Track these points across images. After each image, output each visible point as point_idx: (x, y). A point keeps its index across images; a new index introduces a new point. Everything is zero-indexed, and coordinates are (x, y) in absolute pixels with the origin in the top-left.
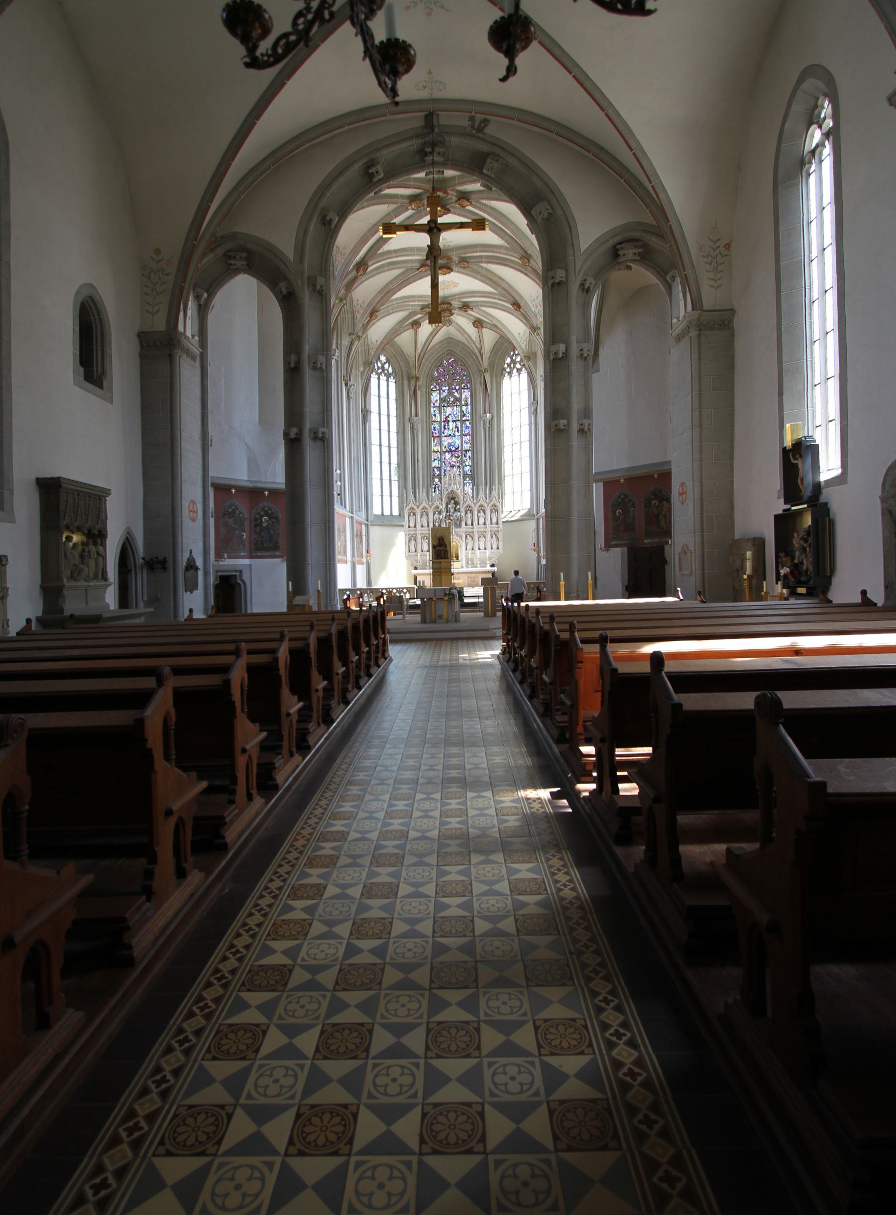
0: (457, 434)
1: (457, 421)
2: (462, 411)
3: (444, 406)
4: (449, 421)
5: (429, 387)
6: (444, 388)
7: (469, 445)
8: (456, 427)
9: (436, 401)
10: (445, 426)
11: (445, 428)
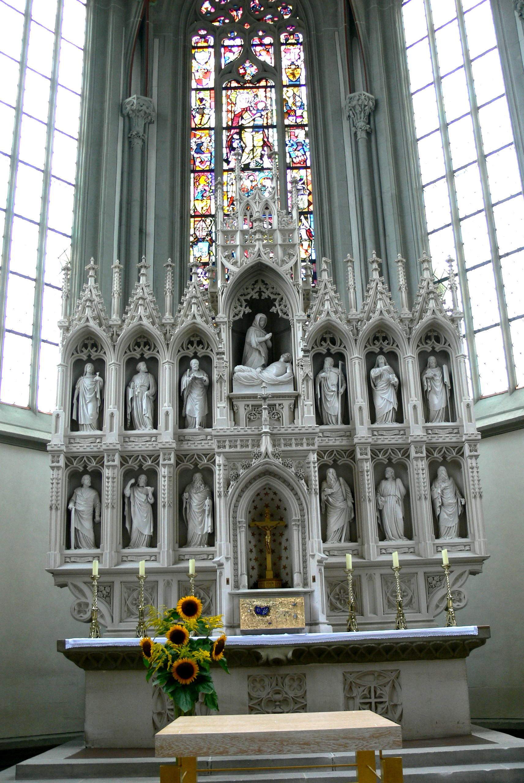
0: (267, 163)
1: (268, 127)
2: (281, 102)
3: (227, 88)
4: (241, 128)
6: (227, 42)
7: (305, 198)
8: (266, 144)
10: (230, 141)
11: (231, 148)
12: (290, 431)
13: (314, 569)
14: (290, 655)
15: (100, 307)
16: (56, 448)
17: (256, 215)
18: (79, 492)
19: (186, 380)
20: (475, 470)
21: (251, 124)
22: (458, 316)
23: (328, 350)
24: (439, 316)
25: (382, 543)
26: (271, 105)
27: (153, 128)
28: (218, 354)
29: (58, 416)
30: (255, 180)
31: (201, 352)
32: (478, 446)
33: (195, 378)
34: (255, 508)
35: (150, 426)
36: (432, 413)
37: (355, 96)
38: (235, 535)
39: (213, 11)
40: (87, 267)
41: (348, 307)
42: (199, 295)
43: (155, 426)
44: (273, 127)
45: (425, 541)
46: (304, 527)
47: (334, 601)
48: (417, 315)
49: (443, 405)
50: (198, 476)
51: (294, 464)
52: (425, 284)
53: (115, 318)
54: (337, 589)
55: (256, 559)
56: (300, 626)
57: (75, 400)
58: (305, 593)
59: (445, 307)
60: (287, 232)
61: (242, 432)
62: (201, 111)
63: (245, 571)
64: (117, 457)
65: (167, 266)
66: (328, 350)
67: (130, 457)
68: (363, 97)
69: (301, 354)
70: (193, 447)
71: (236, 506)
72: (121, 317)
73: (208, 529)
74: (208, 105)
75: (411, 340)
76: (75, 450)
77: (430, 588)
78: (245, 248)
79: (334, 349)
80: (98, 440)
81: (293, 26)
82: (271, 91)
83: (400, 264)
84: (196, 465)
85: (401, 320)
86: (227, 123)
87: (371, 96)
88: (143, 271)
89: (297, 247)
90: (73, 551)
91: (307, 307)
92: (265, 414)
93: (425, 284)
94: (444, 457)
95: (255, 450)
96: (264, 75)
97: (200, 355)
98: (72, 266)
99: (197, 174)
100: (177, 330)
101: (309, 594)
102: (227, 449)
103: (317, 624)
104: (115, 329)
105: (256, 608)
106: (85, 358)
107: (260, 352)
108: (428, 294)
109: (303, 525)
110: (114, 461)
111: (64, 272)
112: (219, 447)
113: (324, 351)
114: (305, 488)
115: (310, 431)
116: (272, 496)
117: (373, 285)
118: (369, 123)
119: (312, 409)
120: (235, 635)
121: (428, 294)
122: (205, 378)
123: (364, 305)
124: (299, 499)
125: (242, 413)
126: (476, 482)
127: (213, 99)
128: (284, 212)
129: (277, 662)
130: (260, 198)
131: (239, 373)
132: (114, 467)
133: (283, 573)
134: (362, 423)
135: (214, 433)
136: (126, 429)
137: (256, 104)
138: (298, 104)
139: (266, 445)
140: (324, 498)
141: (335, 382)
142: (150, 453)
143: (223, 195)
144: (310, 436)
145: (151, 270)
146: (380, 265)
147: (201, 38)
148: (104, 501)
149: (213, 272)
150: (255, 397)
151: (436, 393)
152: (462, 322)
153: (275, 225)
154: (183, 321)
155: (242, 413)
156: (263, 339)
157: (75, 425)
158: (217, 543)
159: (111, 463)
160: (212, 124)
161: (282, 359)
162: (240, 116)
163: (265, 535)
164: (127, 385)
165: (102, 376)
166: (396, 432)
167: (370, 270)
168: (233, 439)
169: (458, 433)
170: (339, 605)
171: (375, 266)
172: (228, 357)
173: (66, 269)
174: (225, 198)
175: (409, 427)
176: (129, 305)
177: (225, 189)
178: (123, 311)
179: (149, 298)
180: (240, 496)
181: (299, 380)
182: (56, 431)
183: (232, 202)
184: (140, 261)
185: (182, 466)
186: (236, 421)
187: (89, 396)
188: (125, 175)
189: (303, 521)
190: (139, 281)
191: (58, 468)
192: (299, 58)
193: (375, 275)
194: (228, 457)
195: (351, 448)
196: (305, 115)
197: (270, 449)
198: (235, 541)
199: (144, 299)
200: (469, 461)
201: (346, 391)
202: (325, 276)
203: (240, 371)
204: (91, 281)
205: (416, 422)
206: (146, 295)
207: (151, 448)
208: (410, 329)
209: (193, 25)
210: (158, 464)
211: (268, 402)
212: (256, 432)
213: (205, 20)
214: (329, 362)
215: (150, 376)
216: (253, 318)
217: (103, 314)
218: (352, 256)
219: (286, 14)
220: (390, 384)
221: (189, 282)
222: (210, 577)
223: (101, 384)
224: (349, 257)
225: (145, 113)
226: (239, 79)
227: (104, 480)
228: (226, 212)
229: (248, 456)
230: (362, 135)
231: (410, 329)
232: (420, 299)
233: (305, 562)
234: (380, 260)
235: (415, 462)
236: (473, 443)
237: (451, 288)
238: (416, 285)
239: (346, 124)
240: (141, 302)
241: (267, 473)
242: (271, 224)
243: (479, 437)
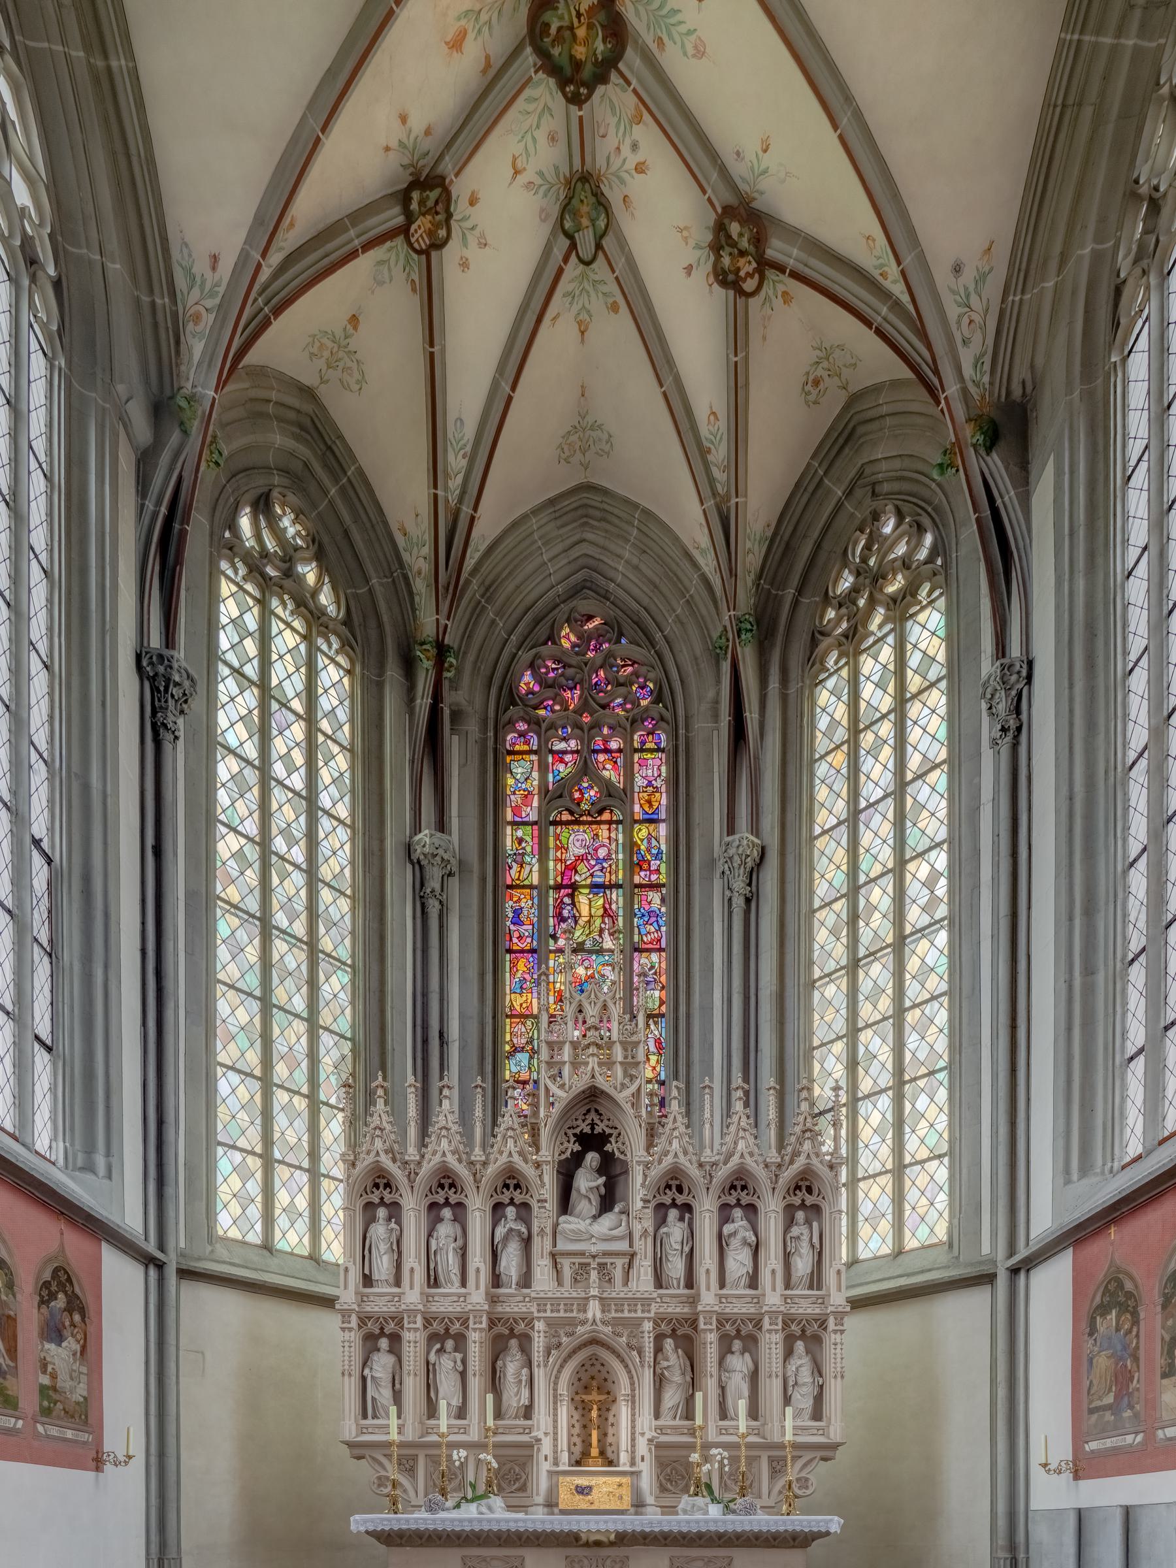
1: (611, 886)
2: (631, 846)
4: (574, 887)
5: (498, 739)
9: (528, 795)
12: (622, 1295)
13: (642, 1447)
14: (612, 1537)
15: (393, 1137)
16: (346, 1307)
17: (590, 1021)
18: (375, 1357)
19: (500, 1231)
20: (839, 1347)
21: (589, 881)
22: (838, 1161)
23: (674, 1200)
24: (815, 1161)
25: (721, 1423)
26: (617, 852)
27: (454, 883)
28: (539, 1201)
29: (346, 1270)
30: (591, 967)
31: (519, 1197)
32: (846, 1319)
33: (511, 1230)
34: (579, 1380)
35: (457, 1283)
36: (794, 1279)
37: (734, 841)
38: (555, 1409)
39: (537, 689)
40: (374, 1085)
41: (702, 1147)
42: (516, 1126)
43: (464, 1284)
44: (618, 886)
45: (772, 1422)
46: (633, 1402)
47: (664, 1482)
48: (787, 1158)
49: (809, 1271)
50: (514, 1343)
51: (625, 1334)
52: (801, 1119)
53: (412, 1153)
54: (669, 1470)
55: (578, 1435)
56: (625, 1507)
57: (366, 1252)
58: (632, 1473)
59: (824, 1149)
60: (629, 1046)
61: (566, 1295)
62: (519, 858)
63: (565, 1448)
64: (419, 1319)
65: (476, 1087)
66: (674, 1200)
67: (435, 1319)
68: (745, 842)
69: (640, 1204)
70: (508, 1309)
71: (557, 1378)
72: (419, 1151)
73: (525, 1401)
74: (529, 849)
75: (776, 1191)
76: (368, 1309)
77: (776, 1472)
78: (575, 1065)
79: (680, 1199)
80: (396, 1299)
81: (653, 719)
82: (617, 829)
83: (772, 1092)
84: (512, 1330)
85: (767, 1166)
86: (555, 879)
87: (756, 840)
88: (446, 1092)
89: (641, 1066)
90: (369, 1421)
91: (650, 1145)
92: (594, 1275)
93: (801, 1119)
94: (803, 1331)
95: (581, 1316)
96: (609, 801)
97: (517, 1201)
98: (355, 1081)
99: (513, 955)
100: (490, 1170)
101: (636, 1474)
102: (548, 1314)
103: (643, 1506)
104: (412, 1166)
105: (577, 1486)
106: (377, 1201)
107: (590, 1200)
108: (804, 1132)
109: (632, 1400)
110: (415, 1323)
111: (344, 1090)
112: (539, 1311)
113: (668, 1201)
114: (638, 1360)
115: (646, 1295)
116: (598, 1367)
117: (735, 1119)
118: (750, 884)
119: (650, 1270)
120: (553, 1514)
121: (804, 1132)
122: (524, 1230)
123: (722, 1144)
124: (629, 1372)
125: (567, 1273)
126: (839, 1360)
127: (536, 840)
128: (627, 1017)
129: (598, 1544)
130: (596, 996)
131: (565, 1225)
132: (416, 1330)
133: (609, 1450)
134: (708, 1289)
135: (533, 1295)
136: (429, 1286)
137: (596, 850)
138: (654, 851)
139: (594, 1310)
140: (658, 1371)
141: (679, 1239)
142: (459, 1315)
143: (548, 990)
144: (646, 1302)
145: (456, 1091)
146: (747, 1093)
147: (520, 736)
148: (405, 1367)
149: (534, 1095)
150: (582, 1254)
151: (801, 1257)
152: (844, 1168)
153: (615, 1037)
154: (497, 1159)
155: (567, 1273)
156: (594, 1184)
157: (368, 1280)
158: (535, 1416)
159: (412, 1326)
160: (535, 879)
161: (616, 1209)
162: (573, 868)
163: (590, 1410)
164: (430, 1235)
165: (399, 1223)
166: (749, 1300)
167: (733, 1099)
168: (555, 1302)
169: (823, 1303)
170: (669, 1486)
171: (740, 1093)
172: (552, 1205)
173: (346, 1085)
174: (551, 993)
175: (764, 1295)
176: (429, 1137)
177: (551, 978)
178: (422, 1144)
179: (455, 1128)
180: (562, 1366)
181: (636, 1235)
182: (345, 1288)
183: (560, 999)
184: (441, 1078)
185: (497, 1330)
186: (560, 1282)
187: (383, 1247)
188: (419, 953)
189: (633, 1396)
190: (441, 1105)
191: (350, 1329)
192: (659, 776)
193: (738, 1106)
194: (550, 1323)
195: (694, 1317)
196: (663, 869)
197: (599, 1315)
198: (555, 1415)
199: (448, 1129)
200: (833, 1336)
201: (692, 1250)
202: (674, 1107)
203: (565, 1222)
204: (380, 1103)
205: (774, 1289)
206: (450, 1125)
207: (459, 1309)
208: (776, 1176)
209: (509, 714)
210: (467, 1327)
211: (597, 1260)
212: (583, 1295)
213: (526, 706)
214: (673, 1214)
215: (457, 1225)
216: (584, 1158)
217: (396, 1147)
218: (711, 1080)
219: (644, 698)
220: (745, 1242)
221: (504, 1109)
222: (526, 1452)
223: (398, 1233)
224: (707, 1083)
225: (443, 859)
226: (574, 807)
227: (405, 1345)
228: (551, 1011)
229: (573, 1322)
230: (739, 902)
231: (776, 1176)
232: (793, 1139)
233: (633, 1440)
234: (746, 1086)
235: (768, 1335)
236: (840, 1316)
237: (834, 1125)
238: (790, 1120)
239: (718, 884)
240: (444, 1132)
241: (594, 1341)
242: (609, 1030)
243: (848, 1309)
